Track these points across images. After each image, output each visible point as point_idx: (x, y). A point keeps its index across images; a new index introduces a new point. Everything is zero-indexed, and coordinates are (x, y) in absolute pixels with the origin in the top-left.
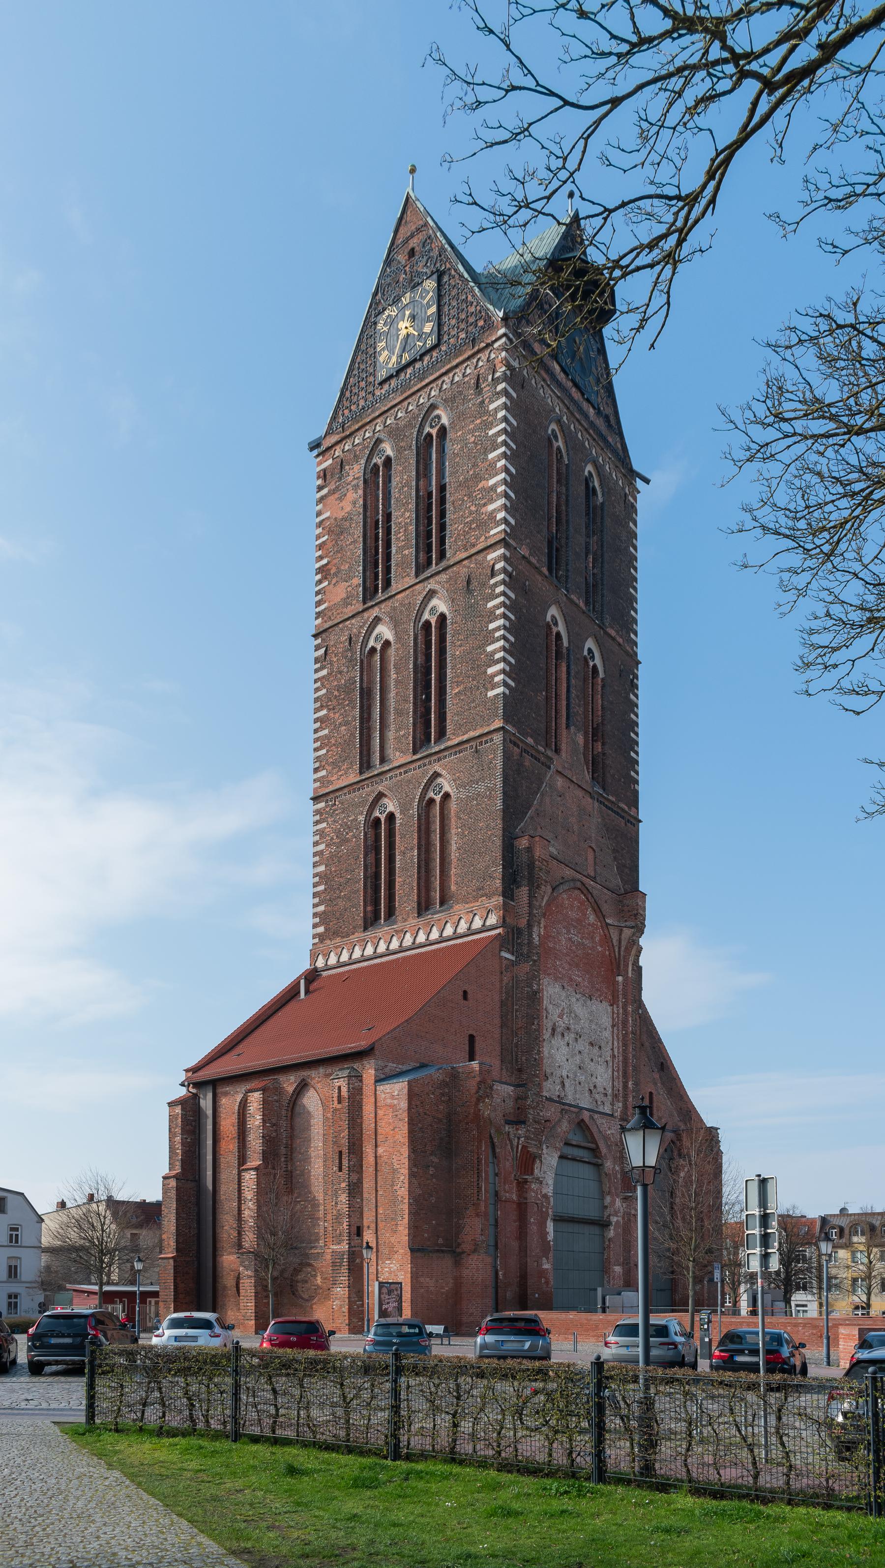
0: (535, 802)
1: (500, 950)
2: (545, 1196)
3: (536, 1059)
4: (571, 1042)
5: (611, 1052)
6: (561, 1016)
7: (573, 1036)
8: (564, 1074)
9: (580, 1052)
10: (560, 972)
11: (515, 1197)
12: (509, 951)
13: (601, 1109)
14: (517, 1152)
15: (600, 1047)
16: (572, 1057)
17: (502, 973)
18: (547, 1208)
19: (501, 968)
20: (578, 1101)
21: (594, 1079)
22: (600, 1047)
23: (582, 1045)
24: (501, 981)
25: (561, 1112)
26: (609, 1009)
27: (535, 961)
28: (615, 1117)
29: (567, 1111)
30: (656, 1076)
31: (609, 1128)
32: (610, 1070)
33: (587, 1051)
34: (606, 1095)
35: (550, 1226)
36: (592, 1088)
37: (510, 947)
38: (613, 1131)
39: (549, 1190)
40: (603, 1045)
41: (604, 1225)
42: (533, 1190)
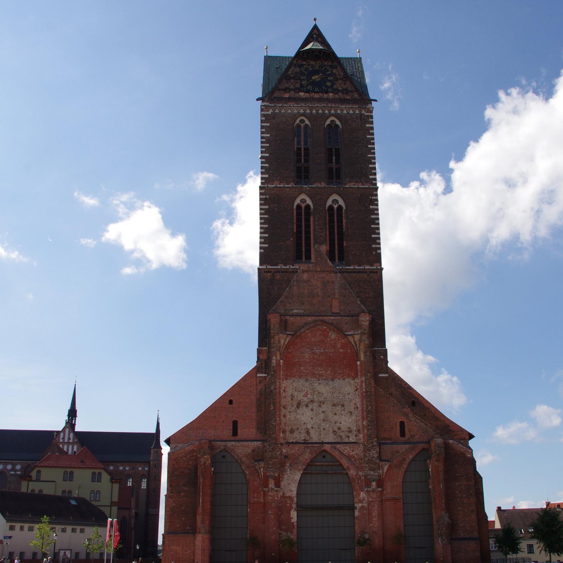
0: (285, 293)
1: (257, 374)
2: (290, 498)
3: (273, 425)
4: (314, 408)
5: (354, 405)
6: (306, 396)
7: (316, 404)
8: (309, 426)
9: (323, 412)
10: (304, 373)
11: (262, 500)
12: (262, 373)
13: (346, 440)
14: (262, 476)
15: (343, 406)
16: (317, 415)
17: (257, 384)
18: (291, 504)
19: (257, 382)
20: (322, 440)
21: (338, 424)
22: (343, 406)
23: (324, 407)
24: (257, 389)
25: (304, 449)
26: (352, 382)
27: (272, 375)
28: (359, 443)
29: (308, 447)
30: (407, 410)
31: (353, 451)
32: (354, 417)
33: (330, 409)
34: (350, 431)
35: (294, 515)
36: (337, 430)
37: (264, 371)
38: (357, 452)
39: (294, 494)
40: (346, 403)
41: (353, 508)
42: (270, 496)
